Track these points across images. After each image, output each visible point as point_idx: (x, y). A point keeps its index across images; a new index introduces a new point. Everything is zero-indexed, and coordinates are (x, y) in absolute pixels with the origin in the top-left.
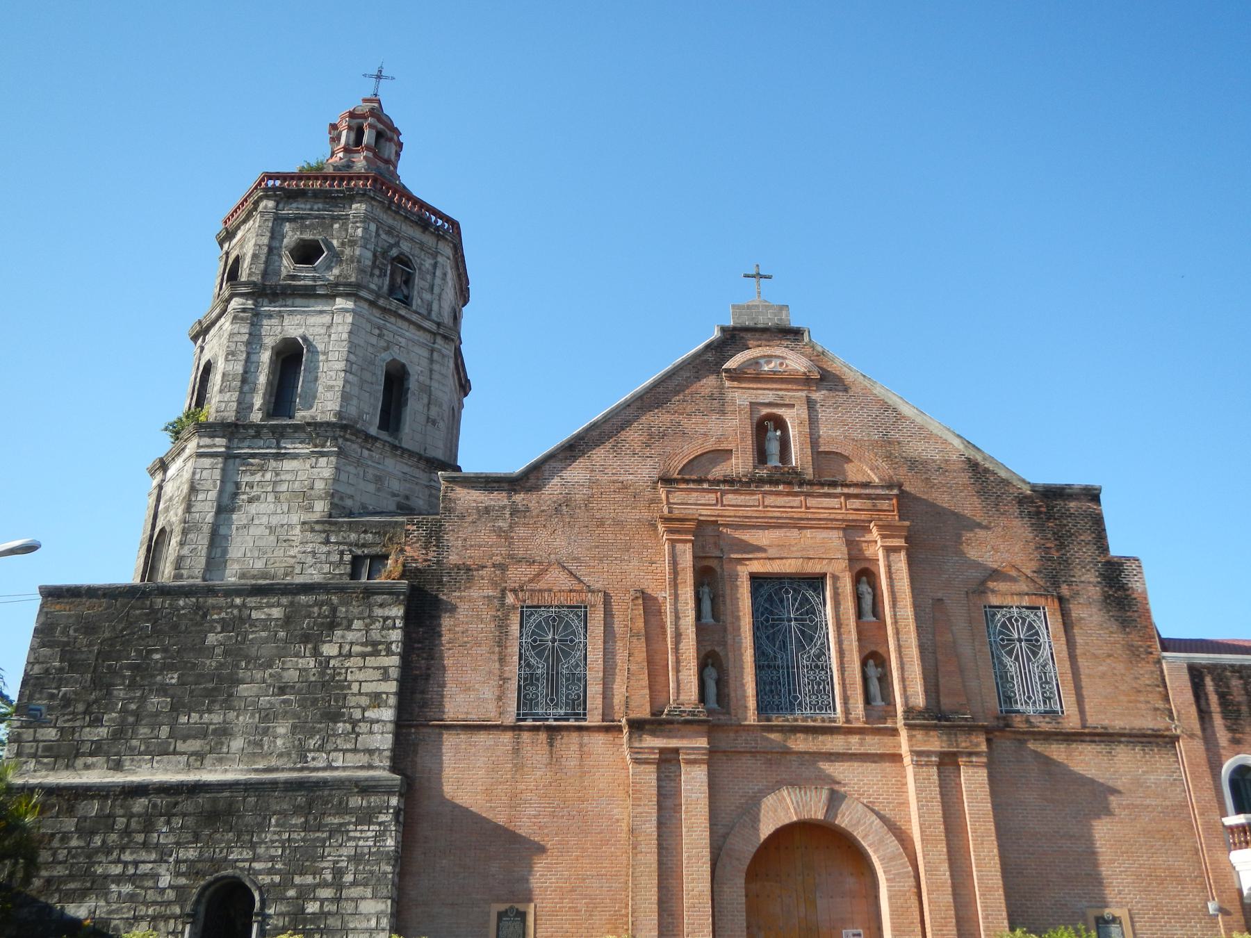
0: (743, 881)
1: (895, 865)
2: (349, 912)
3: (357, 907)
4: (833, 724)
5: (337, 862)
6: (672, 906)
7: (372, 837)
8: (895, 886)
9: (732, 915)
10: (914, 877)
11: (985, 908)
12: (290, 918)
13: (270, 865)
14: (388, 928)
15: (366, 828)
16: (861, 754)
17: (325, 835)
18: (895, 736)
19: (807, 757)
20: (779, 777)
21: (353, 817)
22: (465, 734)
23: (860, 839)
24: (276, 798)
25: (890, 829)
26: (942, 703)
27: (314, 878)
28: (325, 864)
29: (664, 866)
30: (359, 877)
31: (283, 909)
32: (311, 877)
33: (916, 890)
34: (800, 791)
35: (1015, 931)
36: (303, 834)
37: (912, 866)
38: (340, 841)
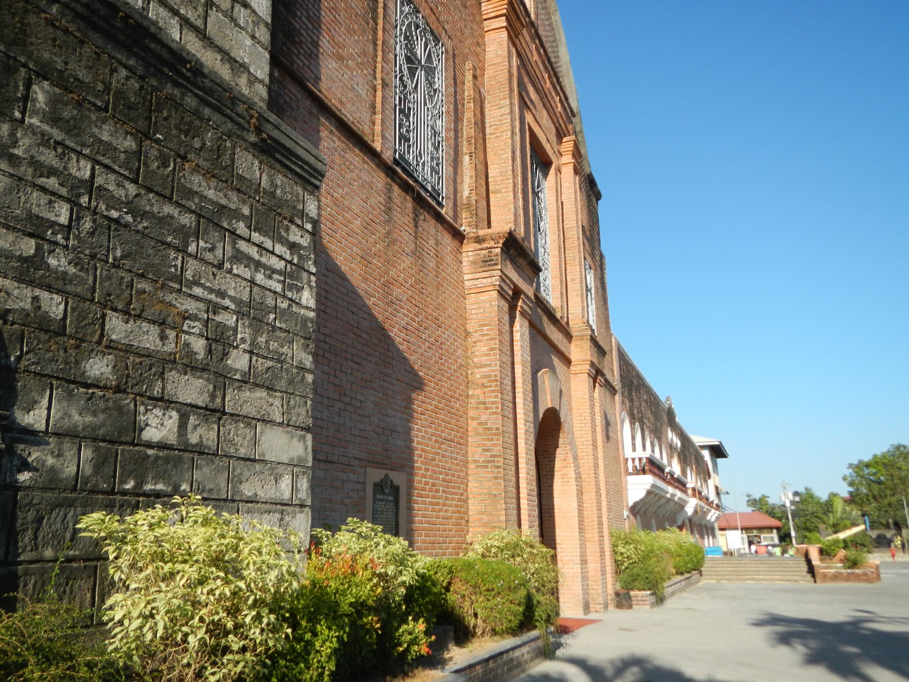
2: (242, 452)
3: (255, 442)
5: (216, 308)
7: (280, 272)
12: (97, 450)
13: (28, 247)
14: (309, 503)
15: (268, 244)
17: (187, 220)
21: (244, 202)
22: (339, 138)
24: (51, 23)
27: (163, 337)
28: (190, 306)
30: (261, 364)
31: (77, 417)
32: (155, 330)
36: (132, 189)
38: (220, 253)
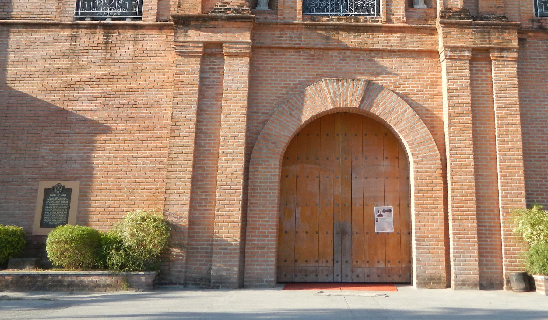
0: (278, 162)
1: (424, 148)
4: (375, 24)
6: (207, 184)
8: (422, 168)
9: (264, 193)
10: (441, 160)
11: (505, 187)
16: (399, 51)
18: (433, 35)
19: (348, 53)
20: (320, 71)
23: (392, 126)
25: (421, 117)
26: (480, 6)
29: (202, 149)
33: (441, 171)
34: (338, 83)
35: (532, 208)
37: (439, 150)
